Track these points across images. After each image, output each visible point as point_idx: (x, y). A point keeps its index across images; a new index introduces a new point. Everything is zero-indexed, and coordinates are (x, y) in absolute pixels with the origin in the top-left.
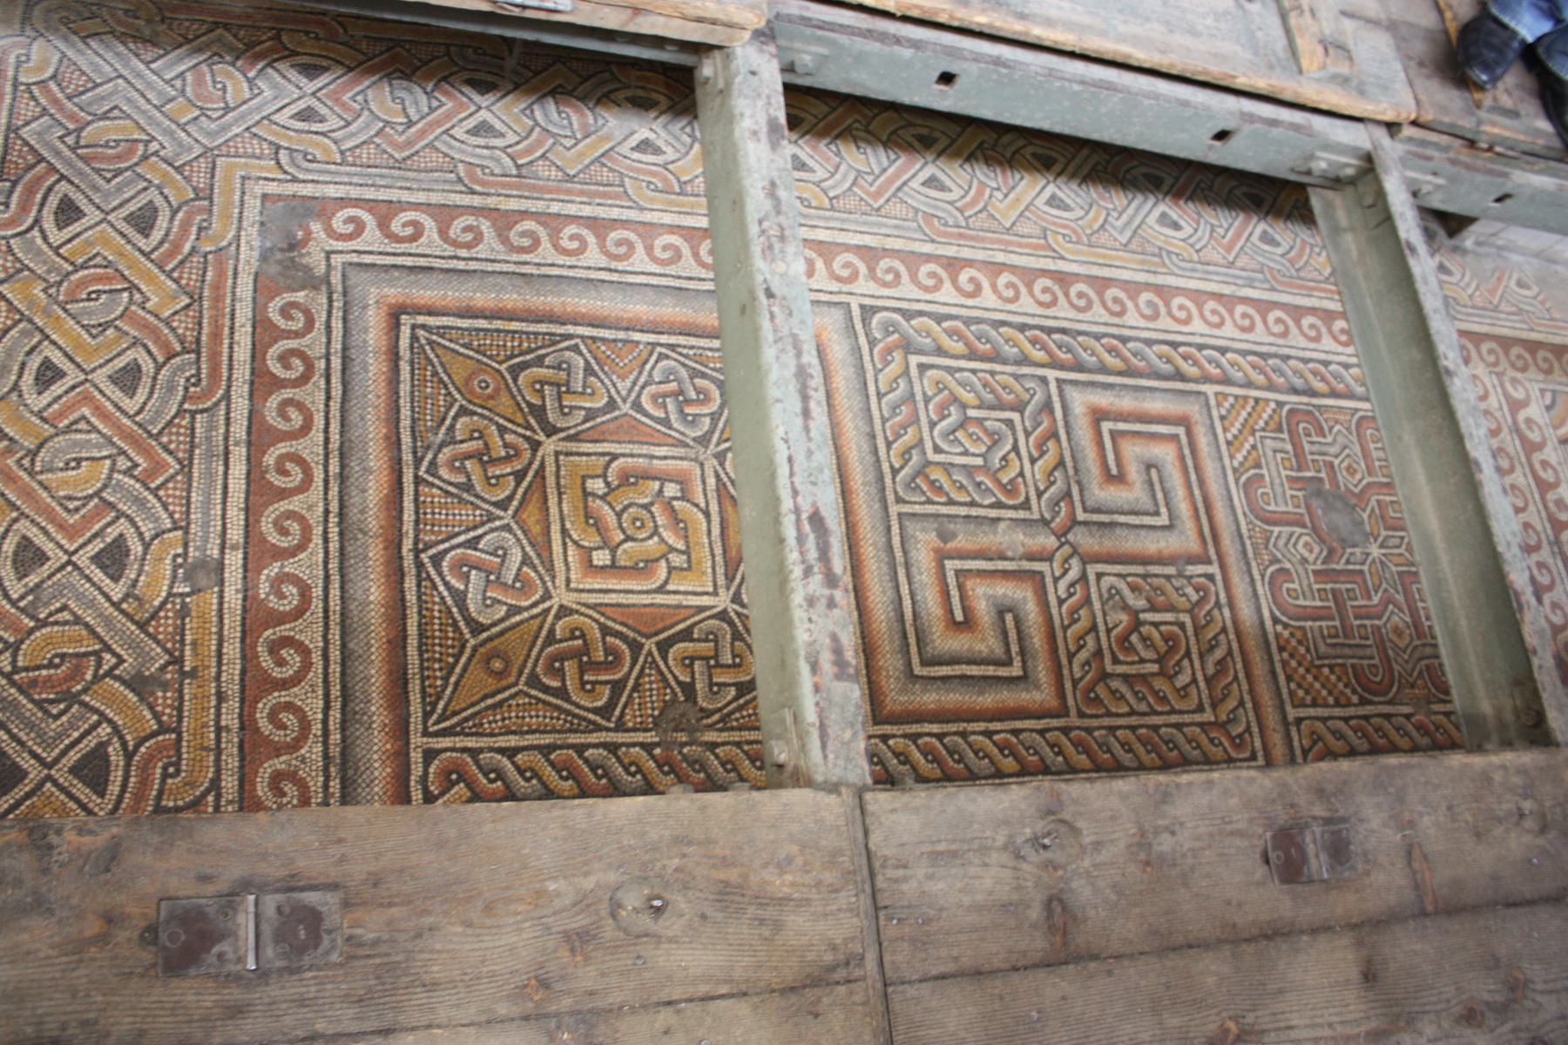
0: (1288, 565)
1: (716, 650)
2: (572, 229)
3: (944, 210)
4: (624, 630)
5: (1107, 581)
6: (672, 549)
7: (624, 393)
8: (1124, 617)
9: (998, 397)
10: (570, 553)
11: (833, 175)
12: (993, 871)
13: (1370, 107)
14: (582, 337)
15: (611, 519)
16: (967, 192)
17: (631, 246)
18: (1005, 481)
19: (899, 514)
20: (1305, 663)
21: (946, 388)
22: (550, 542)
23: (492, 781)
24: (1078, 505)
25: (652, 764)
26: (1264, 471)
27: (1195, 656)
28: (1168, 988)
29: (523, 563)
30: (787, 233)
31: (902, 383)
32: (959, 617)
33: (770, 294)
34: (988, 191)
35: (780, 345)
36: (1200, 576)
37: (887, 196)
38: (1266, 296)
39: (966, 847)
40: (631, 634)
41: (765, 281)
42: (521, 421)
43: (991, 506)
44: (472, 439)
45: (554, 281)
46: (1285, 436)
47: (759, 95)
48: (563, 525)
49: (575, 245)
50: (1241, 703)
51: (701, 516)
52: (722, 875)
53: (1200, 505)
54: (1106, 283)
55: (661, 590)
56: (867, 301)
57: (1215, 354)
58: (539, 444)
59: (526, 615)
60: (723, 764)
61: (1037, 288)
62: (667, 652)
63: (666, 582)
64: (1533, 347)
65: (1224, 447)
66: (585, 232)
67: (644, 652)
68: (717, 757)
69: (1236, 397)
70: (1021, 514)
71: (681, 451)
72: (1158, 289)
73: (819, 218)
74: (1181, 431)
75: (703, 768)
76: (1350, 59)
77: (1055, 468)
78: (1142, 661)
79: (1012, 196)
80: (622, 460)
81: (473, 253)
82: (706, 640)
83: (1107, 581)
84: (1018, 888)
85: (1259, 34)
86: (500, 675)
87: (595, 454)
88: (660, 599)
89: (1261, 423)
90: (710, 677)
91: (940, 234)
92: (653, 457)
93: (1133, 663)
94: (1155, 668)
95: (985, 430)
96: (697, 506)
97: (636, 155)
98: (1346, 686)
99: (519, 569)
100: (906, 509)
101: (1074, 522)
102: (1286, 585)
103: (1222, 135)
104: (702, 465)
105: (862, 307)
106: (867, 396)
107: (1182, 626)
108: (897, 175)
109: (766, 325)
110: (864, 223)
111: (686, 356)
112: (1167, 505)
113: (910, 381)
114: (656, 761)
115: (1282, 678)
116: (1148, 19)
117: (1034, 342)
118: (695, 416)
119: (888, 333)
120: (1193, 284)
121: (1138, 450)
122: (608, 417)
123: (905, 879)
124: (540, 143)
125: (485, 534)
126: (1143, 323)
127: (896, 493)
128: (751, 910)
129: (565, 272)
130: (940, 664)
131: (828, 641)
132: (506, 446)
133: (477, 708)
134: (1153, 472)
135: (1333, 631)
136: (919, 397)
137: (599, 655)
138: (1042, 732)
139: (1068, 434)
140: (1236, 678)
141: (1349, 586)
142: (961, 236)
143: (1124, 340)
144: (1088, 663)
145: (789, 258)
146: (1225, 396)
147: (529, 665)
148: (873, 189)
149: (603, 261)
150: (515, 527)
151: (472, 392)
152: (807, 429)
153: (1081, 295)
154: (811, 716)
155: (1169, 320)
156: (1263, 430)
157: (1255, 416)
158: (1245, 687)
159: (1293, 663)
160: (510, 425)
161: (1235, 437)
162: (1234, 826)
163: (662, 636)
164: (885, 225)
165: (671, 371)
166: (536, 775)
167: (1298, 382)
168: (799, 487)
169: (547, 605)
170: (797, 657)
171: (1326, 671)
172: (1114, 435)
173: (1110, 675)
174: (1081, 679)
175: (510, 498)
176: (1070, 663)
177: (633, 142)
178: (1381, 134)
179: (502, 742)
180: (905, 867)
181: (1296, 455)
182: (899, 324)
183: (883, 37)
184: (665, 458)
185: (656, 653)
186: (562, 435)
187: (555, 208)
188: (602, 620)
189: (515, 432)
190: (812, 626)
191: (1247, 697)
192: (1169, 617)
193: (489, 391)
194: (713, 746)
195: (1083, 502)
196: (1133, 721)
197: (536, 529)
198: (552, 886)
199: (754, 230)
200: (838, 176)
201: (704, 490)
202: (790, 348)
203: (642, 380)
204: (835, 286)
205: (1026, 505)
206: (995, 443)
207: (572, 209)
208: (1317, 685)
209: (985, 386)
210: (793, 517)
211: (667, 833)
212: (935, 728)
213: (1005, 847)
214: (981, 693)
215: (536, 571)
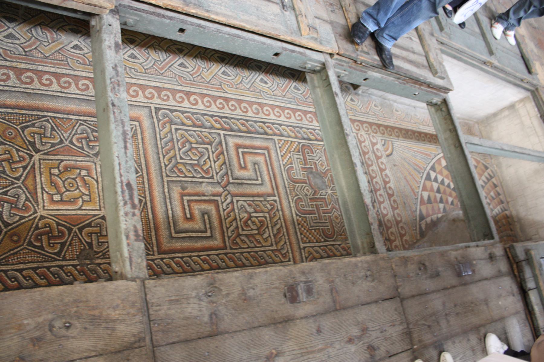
0: (301, 197)
1: (100, 230)
2: (47, 76)
3: (186, 75)
4: (65, 224)
5: (240, 203)
6: (84, 194)
7: (66, 137)
8: (246, 215)
9: (203, 140)
10: (45, 196)
11: (146, 61)
12: (191, 305)
13: (324, 48)
14: (50, 117)
15: (60, 183)
16: (194, 69)
17: (70, 84)
18: (205, 169)
19: (168, 181)
21: (185, 137)
22: (36, 192)
23: (13, 282)
24: (230, 177)
25: (76, 272)
26: (294, 165)
27: (270, 228)
28: (252, 341)
29: (26, 200)
30: (121, 83)
31: (169, 135)
32: (188, 216)
33: (113, 105)
34: (201, 69)
35: (117, 123)
37: (165, 69)
38: (295, 107)
39: (182, 298)
40: (68, 225)
41: (112, 100)
42: (25, 147)
43: (200, 178)
44: (6, 154)
45: (39, 95)
46: (301, 153)
47: (112, 33)
48: (42, 186)
49: (48, 82)
50: (285, 243)
51: (95, 182)
52: (92, 313)
53: (272, 177)
54: (242, 101)
55: (80, 209)
56: (157, 106)
57: (278, 126)
58: (33, 156)
59: (27, 219)
60: (103, 271)
61: (218, 103)
62: (82, 231)
63: (82, 206)
64: (379, 126)
65: (280, 157)
66: (52, 78)
67: (73, 232)
68: (101, 268)
69: (285, 140)
70: (211, 180)
71: (88, 159)
72: (259, 104)
73: (141, 76)
74: (266, 152)
75: (96, 273)
76: (317, 32)
77: (222, 165)
78: (252, 230)
79: (210, 71)
80: (65, 162)
81: (6, 83)
82: (97, 227)
83: (240, 203)
84: (200, 311)
85: (289, 22)
86: (16, 242)
87: (55, 160)
88: (79, 212)
89: (293, 149)
90: (98, 239)
91: (184, 83)
92: (77, 161)
93: (249, 230)
94: (256, 232)
95: (198, 152)
96: (93, 178)
97: (72, 50)
98: (320, 236)
99: (24, 202)
100: (170, 179)
101: (229, 183)
103: (276, 54)
104: (95, 164)
105: (155, 108)
106: (156, 139)
107: (265, 217)
108: (169, 62)
109: (112, 116)
110: (157, 78)
111: (90, 124)
112: (261, 177)
113: (172, 134)
114: (78, 271)
115: (299, 234)
116: (251, 15)
117: (216, 121)
118: (93, 146)
119: (165, 118)
120: (271, 103)
121: (251, 158)
122: (60, 146)
123: (160, 310)
124: (34, 43)
125: (11, 189)
126: (254, 115)
127: (166, 173)
128: (104, 325)
129: (44, 92)
130: (182, 233)
131: (132, 228)
132: (19, 156)
133: (7, 255)
134: (256, 166)
135: (316, 218)
136: (175, 140)
137: (56, 233)
138: (217, 255)
139: (227, 152)
140: (284, 234)
142: (191, 84)
143: (247, 121)
144: (233, 231)
145: (121, 92)
146: (281, 140)
147: (28, 238)
148: (160, 67)
149: (59, 89)
150: (22, 186)
151: (6, 136)
152: (126, 153)
153: (233, 105)
154: (126, 254)
155: (262, 114)
156: (293, 152)
157: (291, 147)
158: (287, 237)
159: (303, 229)
160: (21, 149)
161: (284, 154)
162: (275, 286)
163: (80, 226)
164: (165, 79)
165: (84, 130)
166: (31, 278)
167: (305, 136)
168: (122, 173)
169: (35, 215)
170: (121, 233)
171: (313, 231)
172: (243, 153)
173: (241, 235)
174: (231, 236)
175: (21, 176)
176: (227, 231)
177: (72, 45)
178: (328, 57)
179: (17, 267)
180: (160, 306)
181: (304, 160)
182: (168, 114)
183: (159, 15)
184: (82, 161)
185: (78, 232)
186: (42, 153)
187: (40, 68)
188: (57, 220)
189: (23, 152)
190: (126, 223)
191: (287, 241)
192: (261, 214)
193: (12, 136)
194: (99, 265)
195: (232, 176)
196: (249, 250)
197: (31, 188)
198: (26, 322)
199: (108, 82)
200: (148, 61)
201: (96, 173)
202: (120, 124)
203: (73, 133)
204: (146, 100)
205: (212, 177)
206: (202, 156)
207: (47, 69)
208: (310, 236)
209: (198, 136)
210: (120, 184)
211: (71, 299)
212: (180, 255)
213: (195, 297)
214: (196, 242)
215: (31, 203)
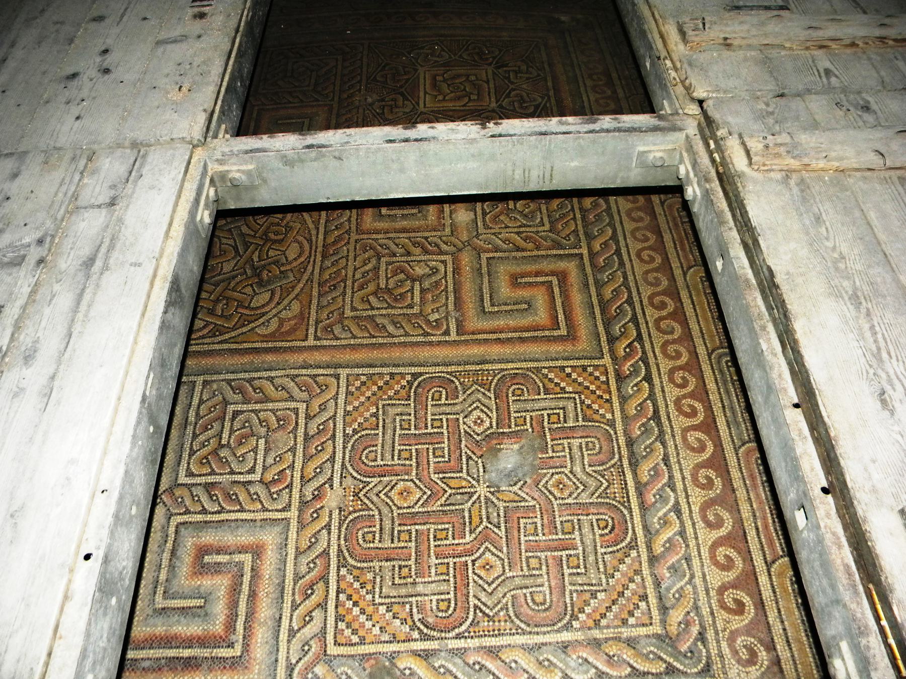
20: (380, 393)
26: (542, 396)
50: (354, 337)
69: (607, 383)
101: (478, 251)
102: (444, 392)
134: (525, 306)
141: (446, 452)
158: (365, 341)
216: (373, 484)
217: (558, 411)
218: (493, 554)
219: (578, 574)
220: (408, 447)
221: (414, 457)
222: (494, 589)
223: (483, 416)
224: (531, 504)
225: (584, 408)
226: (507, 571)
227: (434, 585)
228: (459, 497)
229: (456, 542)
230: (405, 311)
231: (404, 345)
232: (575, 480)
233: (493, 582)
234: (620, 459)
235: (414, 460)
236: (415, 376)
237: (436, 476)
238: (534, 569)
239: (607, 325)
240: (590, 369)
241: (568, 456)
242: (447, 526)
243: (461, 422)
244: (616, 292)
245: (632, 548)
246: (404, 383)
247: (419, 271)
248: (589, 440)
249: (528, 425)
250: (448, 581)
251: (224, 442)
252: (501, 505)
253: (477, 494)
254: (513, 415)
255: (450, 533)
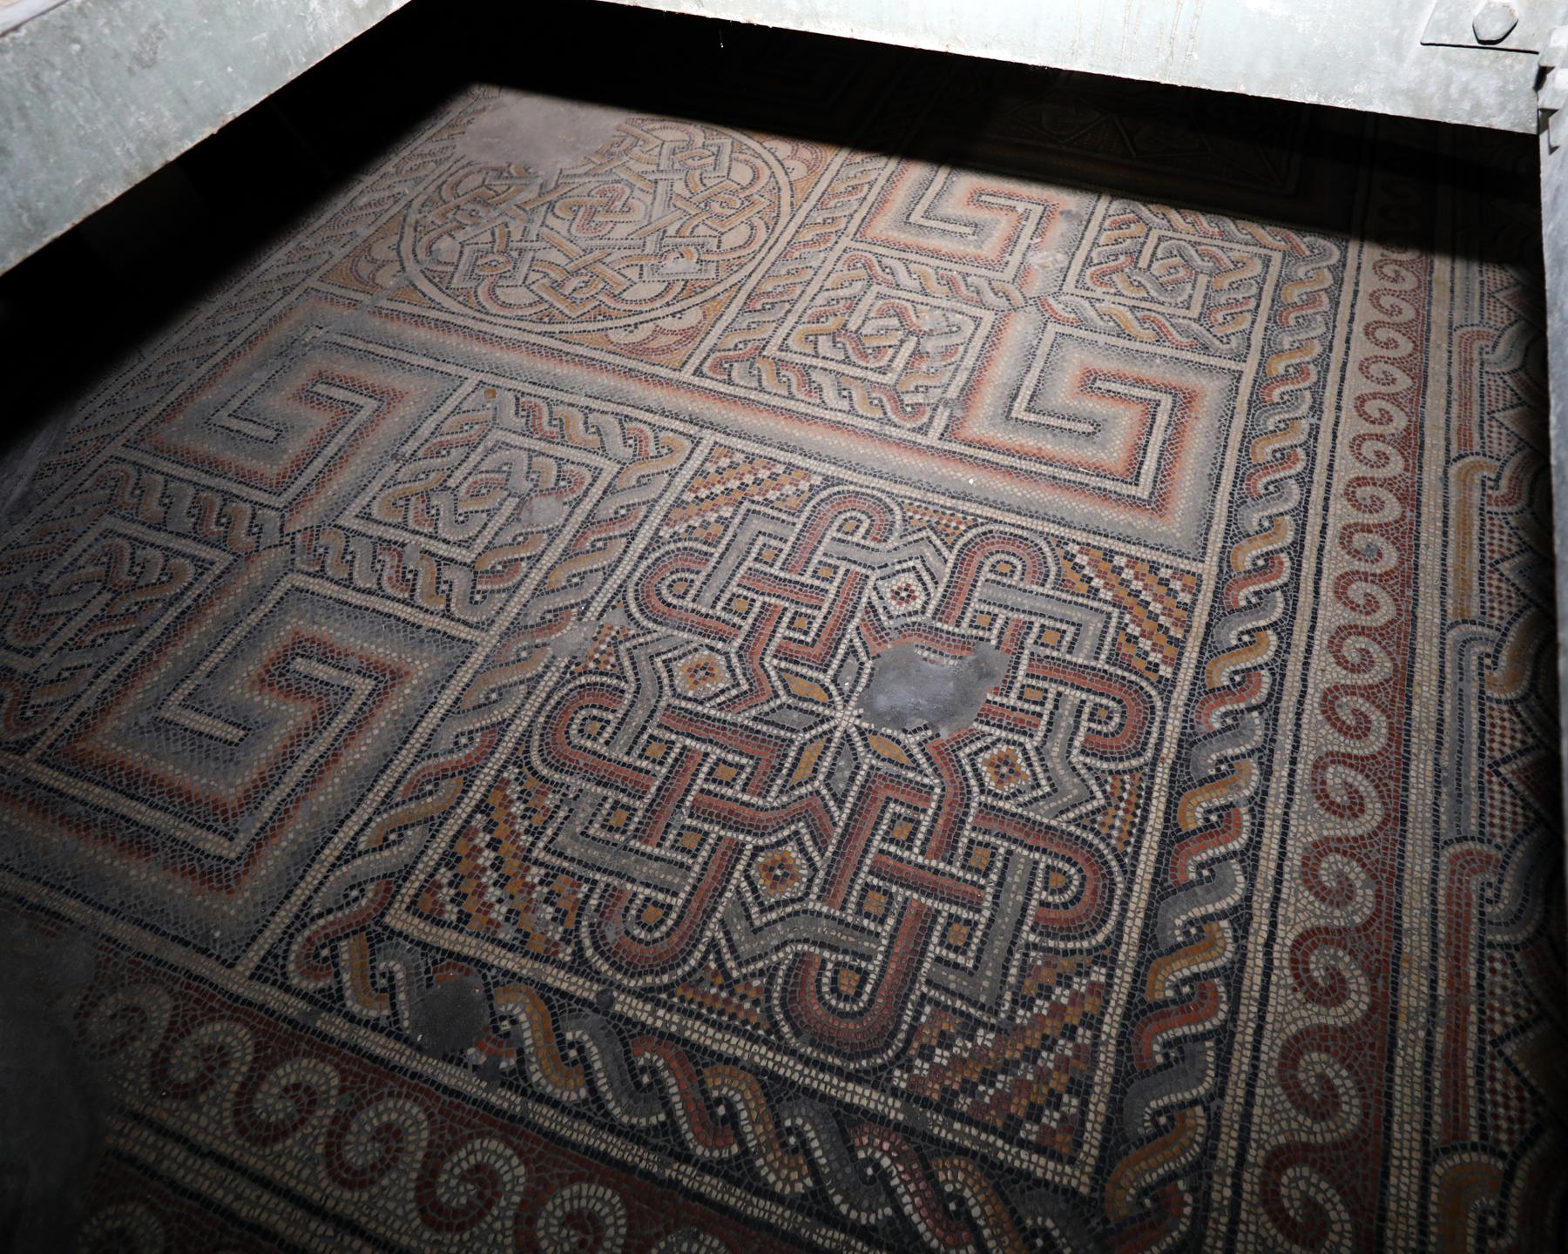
20: (753, 489)
36: (932, 418)
69: (1189, 609)
102: (866, 525)
107: (882, 371)
121: (1125, 422)
140: (791, 397)
141: (815, 626)
158: (776, 401)
216: (655, 636)
217: (1064, 627)
218: (803, 850)
219: (956, 966)
220: (750, 595)
221: (752, 616)
222: (768, 924)
223: (917, 588)
224: (926, 781)
225: (1122, 639)
226: (813, 897)
227: (656, 865)
228: (795, 715)
229: (746, 798)
230: (870, 375)
231: (837, 426)
232: (1038, 770)
233: (771, 908)
234: (1154, 763)
235: (750, 620)
236: (829, 481)
237: (775, 662)
238: (868, 916)
239: (1237, 503)
240: (1164, 573)
241: (1046, 718)
242: (744, 761)
243: (871, 583)
244: (1284, 457)
245: (1099, 960)
246: (804, 486)
247: (926, 321)
248: (1104, 701)
249: (995, 632)
250: (689, 868)
251: (451, 483)
252: (868, 761)
253: (832, 724)
254: (974, 604)
255: (744, 776)
